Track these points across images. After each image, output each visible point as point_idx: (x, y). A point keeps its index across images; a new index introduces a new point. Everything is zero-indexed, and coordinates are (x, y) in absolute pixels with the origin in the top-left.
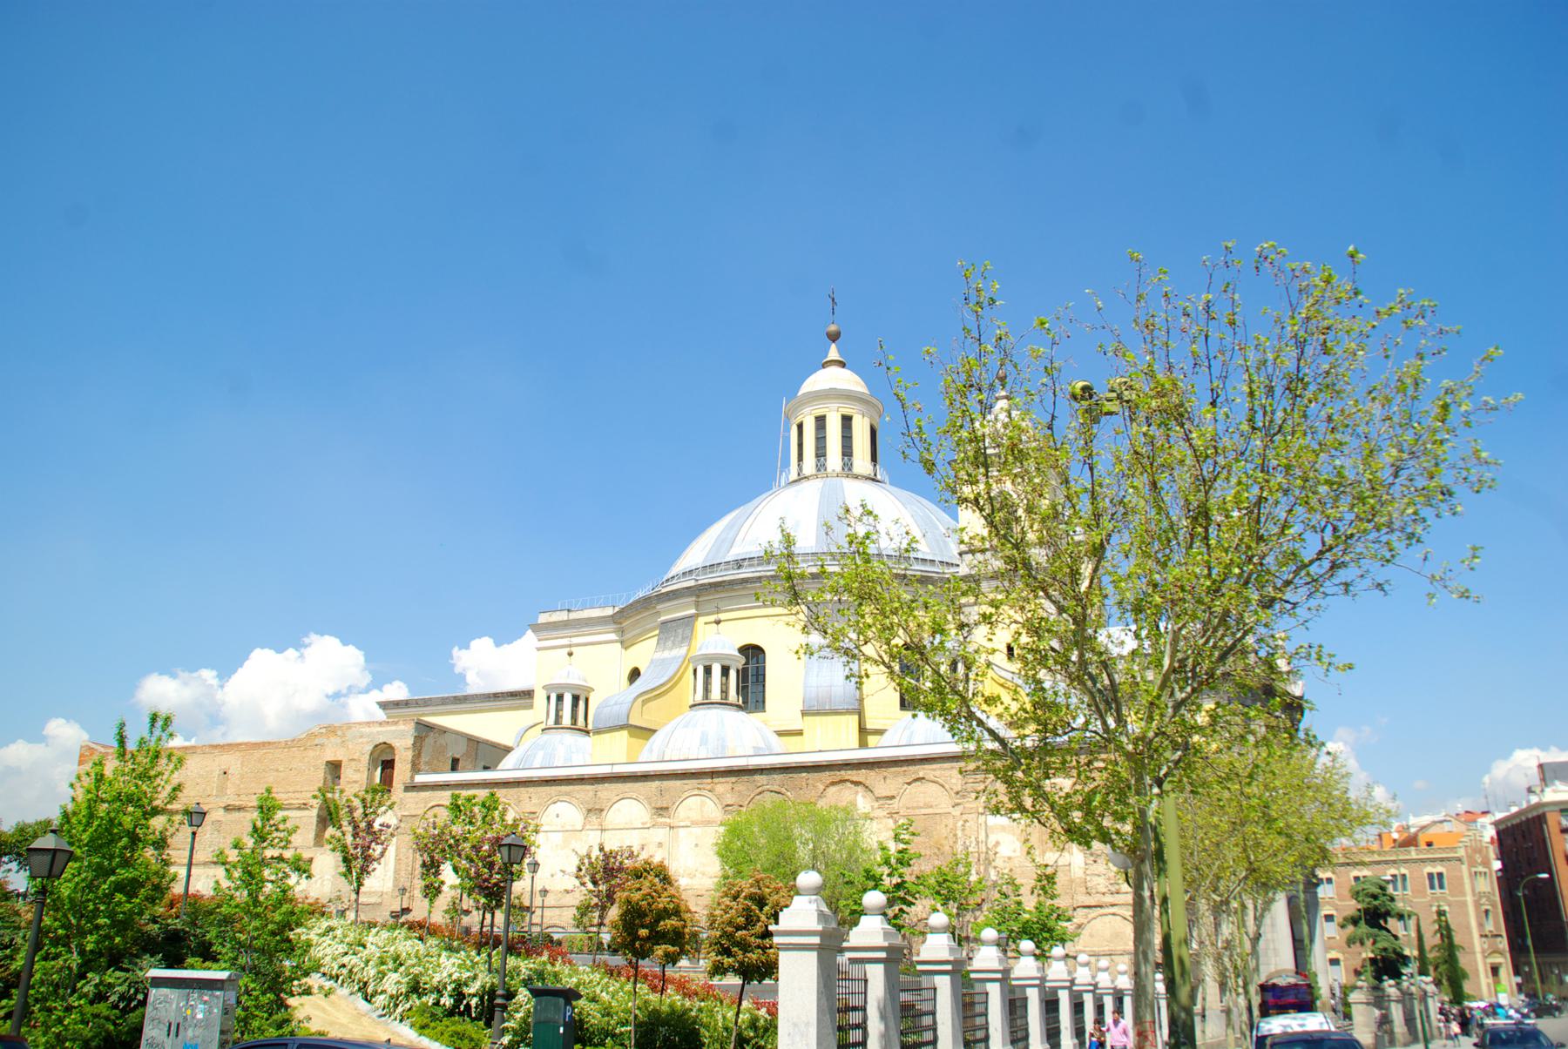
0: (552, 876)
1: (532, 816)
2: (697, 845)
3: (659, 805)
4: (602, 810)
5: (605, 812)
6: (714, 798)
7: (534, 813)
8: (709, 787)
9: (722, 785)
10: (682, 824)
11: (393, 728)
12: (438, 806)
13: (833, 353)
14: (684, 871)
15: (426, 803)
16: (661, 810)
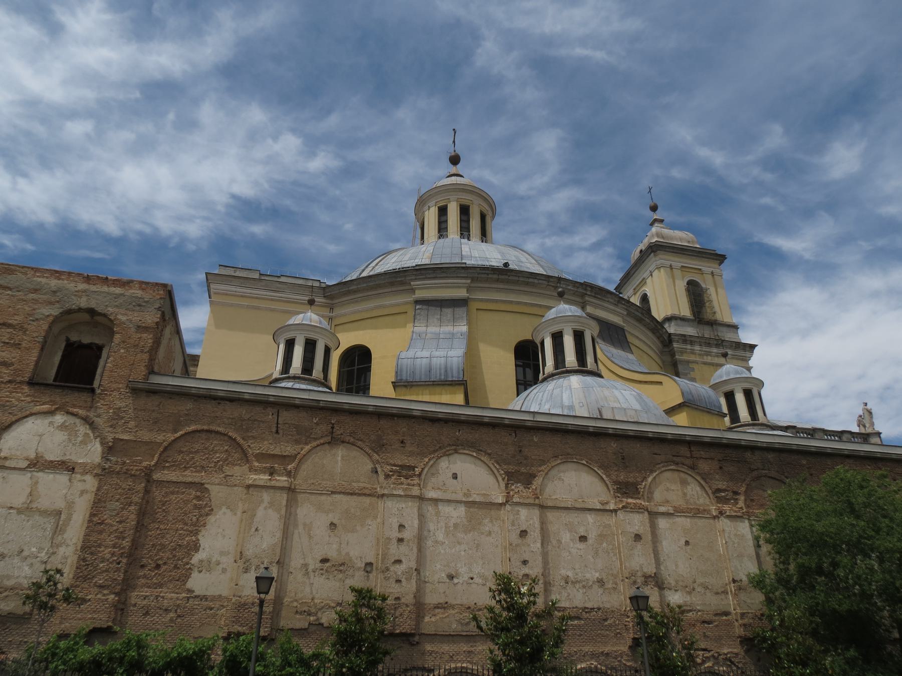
0: (451, 577)
1: (404, 472)
2: (687, 543)
5: (537, 482)
6: (699, 478)
7: (413, 468)
10: (662, 509)
11: (118, 290)
14: (677, 582)
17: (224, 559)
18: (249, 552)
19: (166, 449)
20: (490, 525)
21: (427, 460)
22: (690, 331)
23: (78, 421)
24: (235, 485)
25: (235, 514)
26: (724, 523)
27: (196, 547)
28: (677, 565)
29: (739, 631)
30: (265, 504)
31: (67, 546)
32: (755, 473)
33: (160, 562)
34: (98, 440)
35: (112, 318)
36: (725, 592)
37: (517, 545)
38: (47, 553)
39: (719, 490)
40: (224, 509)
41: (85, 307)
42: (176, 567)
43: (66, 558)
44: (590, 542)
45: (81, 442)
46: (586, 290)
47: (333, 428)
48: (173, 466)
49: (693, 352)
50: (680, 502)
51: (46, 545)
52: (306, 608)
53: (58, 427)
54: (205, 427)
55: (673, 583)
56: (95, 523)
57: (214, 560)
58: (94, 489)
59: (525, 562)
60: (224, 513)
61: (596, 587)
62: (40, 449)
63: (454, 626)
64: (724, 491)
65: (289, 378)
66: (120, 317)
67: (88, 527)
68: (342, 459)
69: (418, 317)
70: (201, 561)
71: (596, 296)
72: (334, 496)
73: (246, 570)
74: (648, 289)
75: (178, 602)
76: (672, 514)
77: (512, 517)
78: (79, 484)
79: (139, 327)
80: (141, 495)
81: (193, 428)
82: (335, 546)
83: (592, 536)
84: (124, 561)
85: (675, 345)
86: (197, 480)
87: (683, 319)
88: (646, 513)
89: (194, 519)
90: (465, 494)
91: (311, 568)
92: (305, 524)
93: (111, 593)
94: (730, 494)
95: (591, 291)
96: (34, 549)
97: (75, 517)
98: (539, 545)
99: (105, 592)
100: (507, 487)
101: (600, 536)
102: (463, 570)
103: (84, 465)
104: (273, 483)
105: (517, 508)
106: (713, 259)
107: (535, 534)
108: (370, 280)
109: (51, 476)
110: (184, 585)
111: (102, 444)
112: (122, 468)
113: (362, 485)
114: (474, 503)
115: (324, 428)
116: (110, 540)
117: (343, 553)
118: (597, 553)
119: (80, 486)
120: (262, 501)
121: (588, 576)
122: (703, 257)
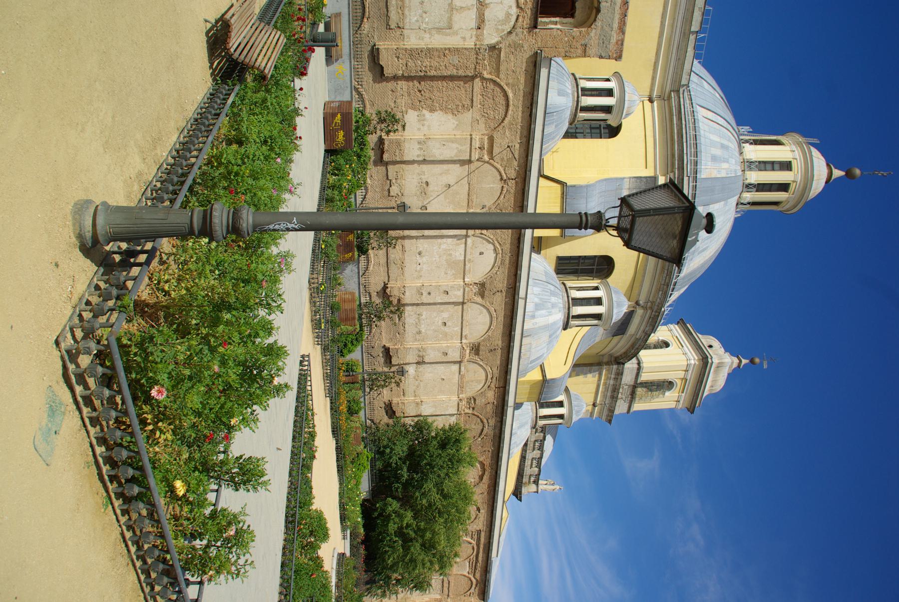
0: (420, 253)
3: (482, 348)
4: (483, 297)
5: (479, 299)
6: (482, 390)
8: (493, 386)
9: (491, 396)
10: (463, 368)
11: (616, 25)
12: (508, 106)
13: (837, 173)
15: (513, 86)
16: (476, 349)
17: (426, 128)
18: (430, 143)
19: (495, 82)
20: (451, 274)
21: (492, 237)
22: (628, 378)
23: (512, 23)
24: (472, 127)
25: (453, 130)
26: (455, 398)
27: (432, 110)
28: (429, 373)
29: (395, 400)
30: (460, 148)
31: (430, 38)
32: (485, 421)
33: (422, 92)
34: (500, 38)
35: (593, 26)
36: (415, 396)
37: (439, 289)
38: (425, 28)
39: (475, 400)
40: (457, 122)
41: (601, 6)
42: (420, 101)
43: (423, 39)
44: (443, 328)
45: (498, 29)
46: (656, 312)
47: (512, 179)
48: (484, 87)
49: (608, 378)
50: (467, 379)
51: (430, 26)
52: (399, 177)
53: (508, 12)
54: (511, 103)
55: (420, 370)
56: (444, 52)
57: (425, 123)
58: (466, 47)
59: (429, 294)
60: (454, 123)
61: (417, 330)
62: (492, 5)
63: (393, 256)
64: (475, 403)
65: (578, 97)
66: (594, 31)
67: (442, 49)
68: (491, 187)
69: (638, 181)
70: (424, 115)
71: (651, 319)
72: (467, 185)
73: (419, 143)
74: (673, 348)
75: (400, 107)
76: (460, 374)
77: (456, 286)
78: (469, 35)
79: (586, 45)
80: (463, 74)
81: (511, 95)
82: (436, 188)
83: (446, 329)
84: (422, 74)
85: (615, 367)
86: (475, 104)
87: (638, 375)
88: (459, 360)
89: (450, 107)
90: (470, 260)
91: (423, 177)
92: (448, 170)
93: (403, 71)
94: (473, 405)
95: (655, 315)
96: (427, 20)
97: (448, 37)
98: (440, 301)
99: (404, 68)
100: (475, 283)
101: (446, 333)
102: (424, 259)
103: (482, 35)
104: (473, 150)
105: (462, 290)
106: (692, 404)
107: (446, 299)
108: (680, 136)
109: (474, 17)
110: (410, 108)
111: (498, 43)
112: (480, 59)
113: (475, 200)
114: (465, 265)
115: (513, 174)
116: (434, 64)
117: (432, 194)
118: (436, 331)
119: (468, 35)
120: (462, 146)
121: (423, 326)
122: (694, 396)
